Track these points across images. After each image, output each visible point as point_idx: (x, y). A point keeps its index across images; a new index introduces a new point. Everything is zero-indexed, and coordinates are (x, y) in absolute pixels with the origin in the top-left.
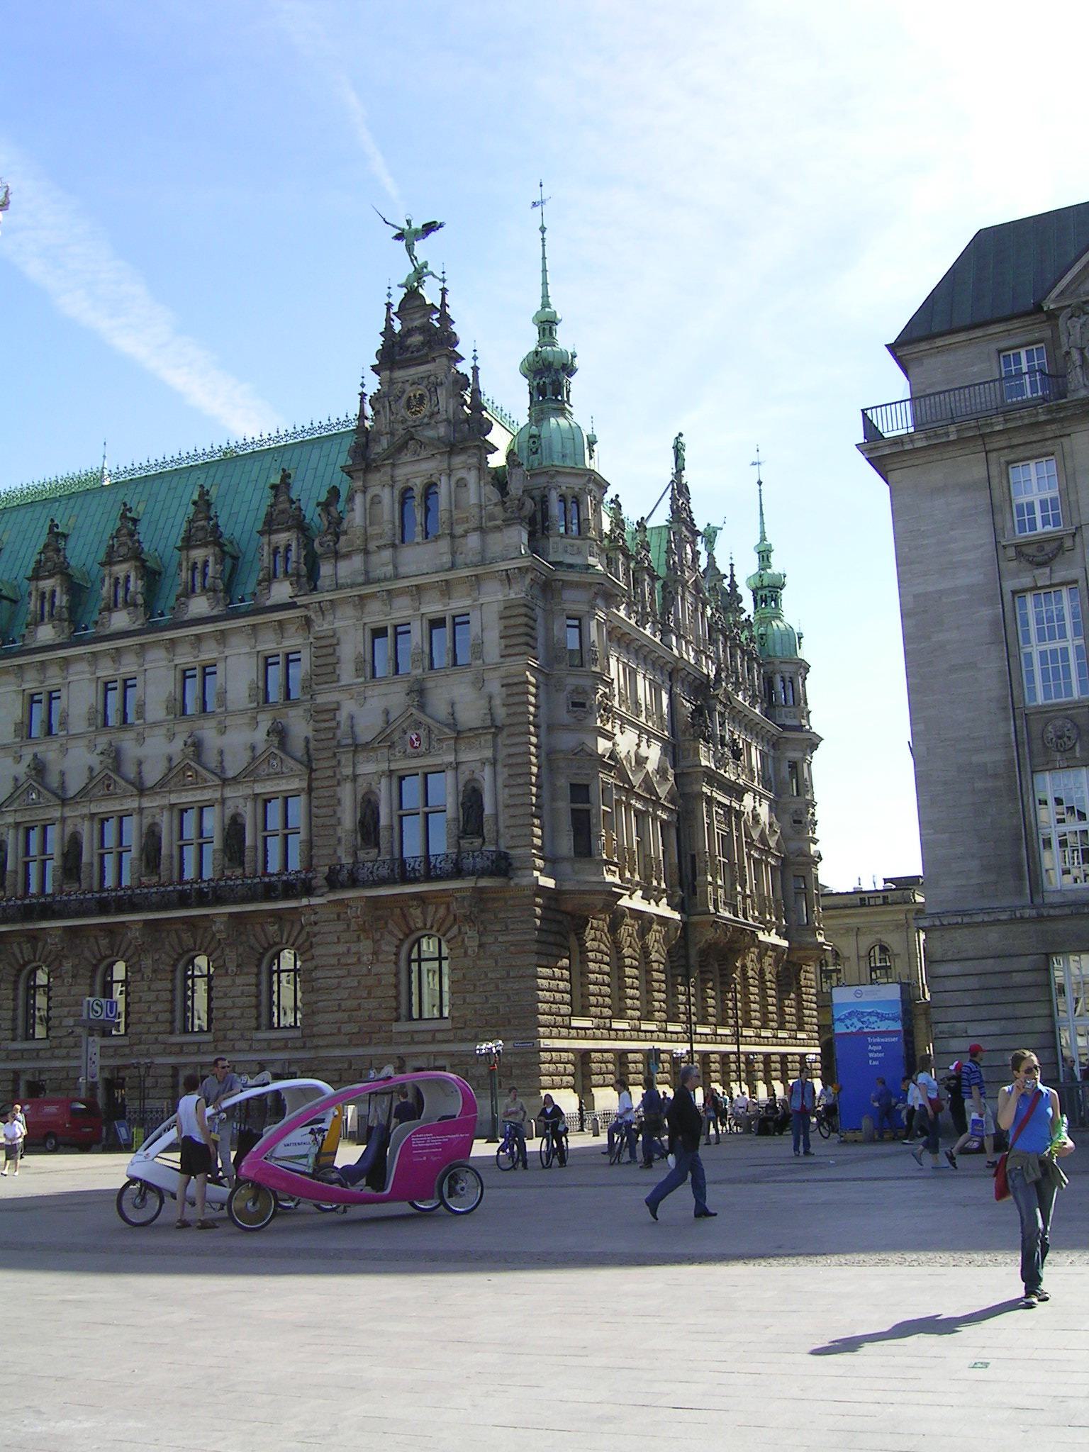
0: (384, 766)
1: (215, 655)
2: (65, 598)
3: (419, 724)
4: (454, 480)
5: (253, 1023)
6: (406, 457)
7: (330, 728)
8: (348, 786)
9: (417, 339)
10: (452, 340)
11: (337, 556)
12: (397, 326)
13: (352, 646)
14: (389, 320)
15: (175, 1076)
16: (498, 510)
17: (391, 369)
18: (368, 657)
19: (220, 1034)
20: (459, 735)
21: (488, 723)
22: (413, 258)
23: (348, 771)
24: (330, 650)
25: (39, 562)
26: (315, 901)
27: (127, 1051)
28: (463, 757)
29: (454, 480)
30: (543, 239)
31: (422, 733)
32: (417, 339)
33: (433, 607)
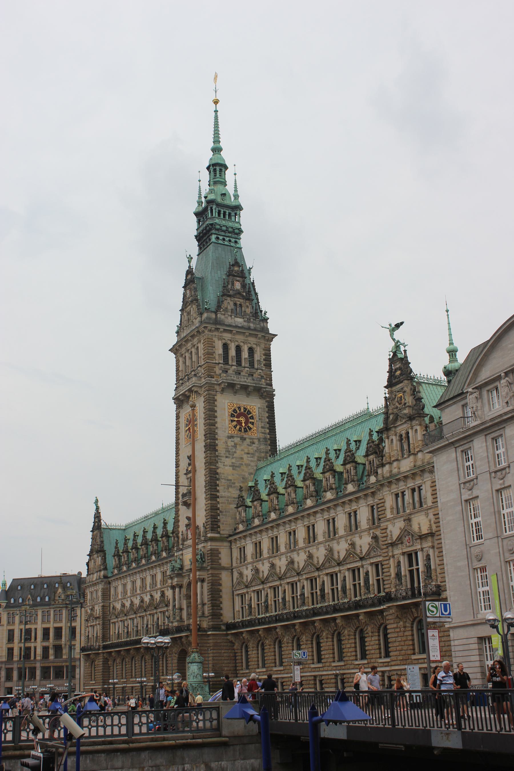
0: (401, 551)
1: (356, 507)
2: (313, 487)
5: (378, 656)
8: (392, 559)
9: (398, 373)
11: (383, 465)
15: (336, 678)
18: (395, 506)
19: (369, 660)
20: (422, 537)
21: (429, 531)
22: (394, 340)
23: (390, 554)
24: (382, 505)
27: (344, 667)
28: (424, 546)
29: (414, 430)
30: (448, 315)
31: (410, 536)
32: (398, 373)
33: (411, 484)
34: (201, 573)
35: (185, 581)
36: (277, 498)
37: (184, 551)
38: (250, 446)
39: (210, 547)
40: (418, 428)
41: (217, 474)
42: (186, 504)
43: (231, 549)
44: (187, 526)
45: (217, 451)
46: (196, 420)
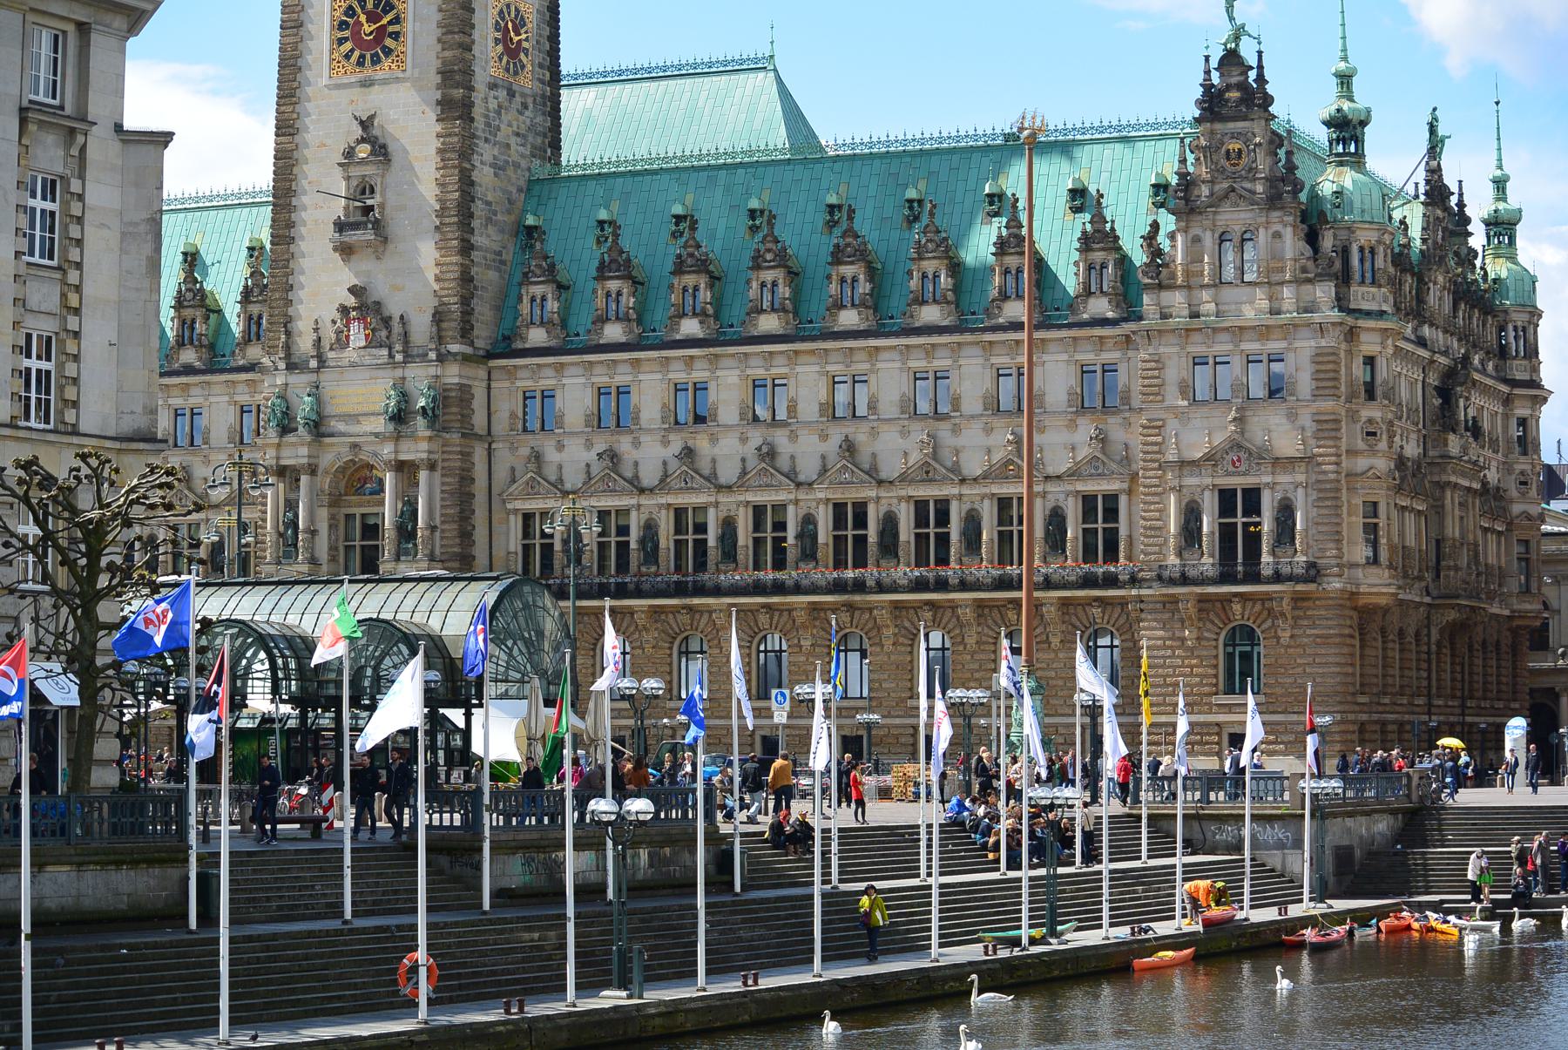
0: (1208, 481)
3: (1240, 447)
4: (1270, 232)
6: (1226, 207)
7: (1156, 444)
9: (1234, 95)
10: (1268, 100)
12: (1216, 78)
13: (1175, 371)
14: (1208, 72)
16: (1310, 264)
17: (1212, 121)
22: (1231, 19)
25: (837, 246)
26: (1144, 592)
33: (1251, 346)
34: (435, 446)
35: (333, 455)
36: (711, 286)
37: (326, 377)
38: (521, 113)
39: (456, 380)
40: (1288, 233)
41: (472, 184)
42: (346, 251)
43: (489, 388)
44: (344, 310)
45: (472, 120)
46: (397, 20)
